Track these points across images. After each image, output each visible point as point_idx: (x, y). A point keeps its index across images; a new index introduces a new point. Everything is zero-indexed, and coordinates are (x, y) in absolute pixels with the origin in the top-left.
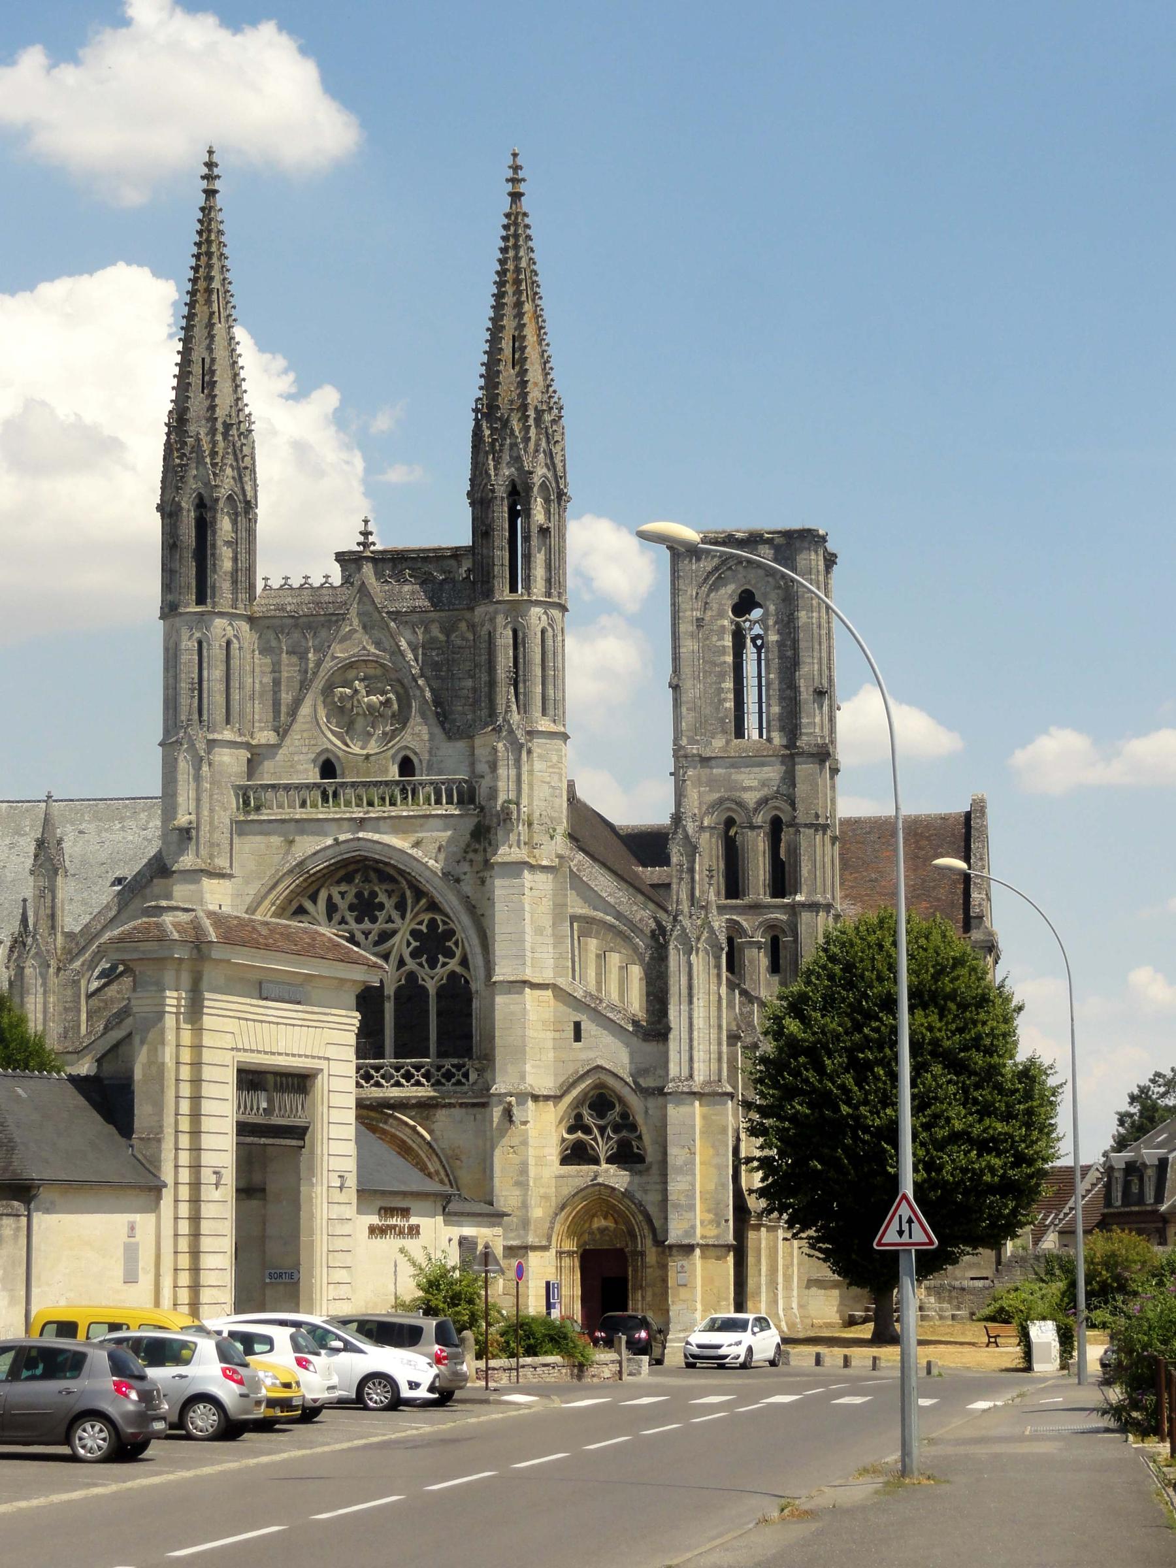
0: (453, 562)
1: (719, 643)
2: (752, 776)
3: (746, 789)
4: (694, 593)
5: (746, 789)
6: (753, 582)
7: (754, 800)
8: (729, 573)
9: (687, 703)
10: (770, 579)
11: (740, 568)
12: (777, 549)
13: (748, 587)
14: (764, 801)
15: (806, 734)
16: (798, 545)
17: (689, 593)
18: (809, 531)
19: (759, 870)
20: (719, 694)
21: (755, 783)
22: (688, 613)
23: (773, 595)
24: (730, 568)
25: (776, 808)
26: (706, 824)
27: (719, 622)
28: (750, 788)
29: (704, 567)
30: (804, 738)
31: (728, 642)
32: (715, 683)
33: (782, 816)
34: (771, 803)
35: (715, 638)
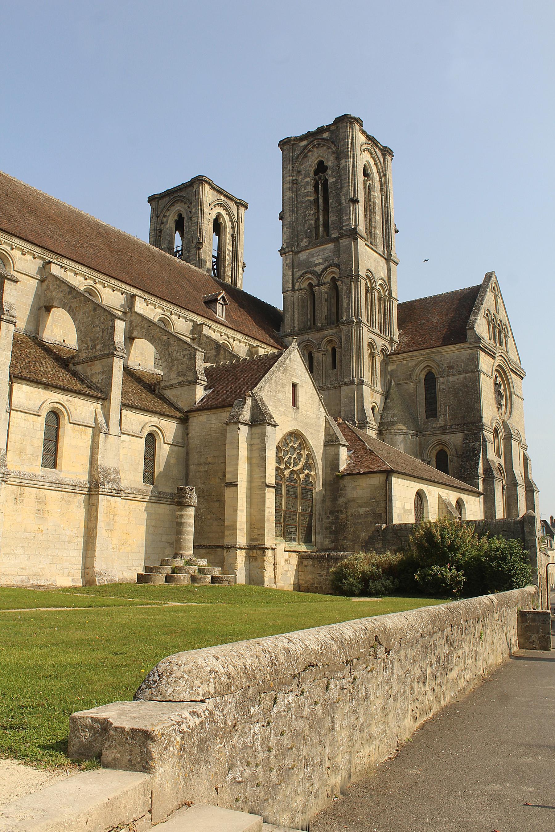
0: (191, 188)
1: (305, 191)
2: (320, 257)
3: (316, 265)
4: (291, 167)
5: (316, 265)
6: (321, 155)
7: (321, 271)
8: (310, 154)
9: (286, 225)
10: (330, 150)
11: (315, 149)
12: (332, 132)
13: (321, 159)
14: (325, 269)
15: (345, 226)
16: (340, 126)
17: (288, 168)
18: (345, 115)
19: (323, 311)
20: (305, 218)
21: (321, 261)
22: (288, 178)
23: (332, 158)
24: (310, 151)
25: (333, 272)
26: (296, 288)
27: (306, 180)
28: (319, 264)
29: (297, 154)
30: (344, 228)
31: (311, 189)
32: (303, 212)
33: (336, 276)
34: (329, 270)
35: (303, 190)
